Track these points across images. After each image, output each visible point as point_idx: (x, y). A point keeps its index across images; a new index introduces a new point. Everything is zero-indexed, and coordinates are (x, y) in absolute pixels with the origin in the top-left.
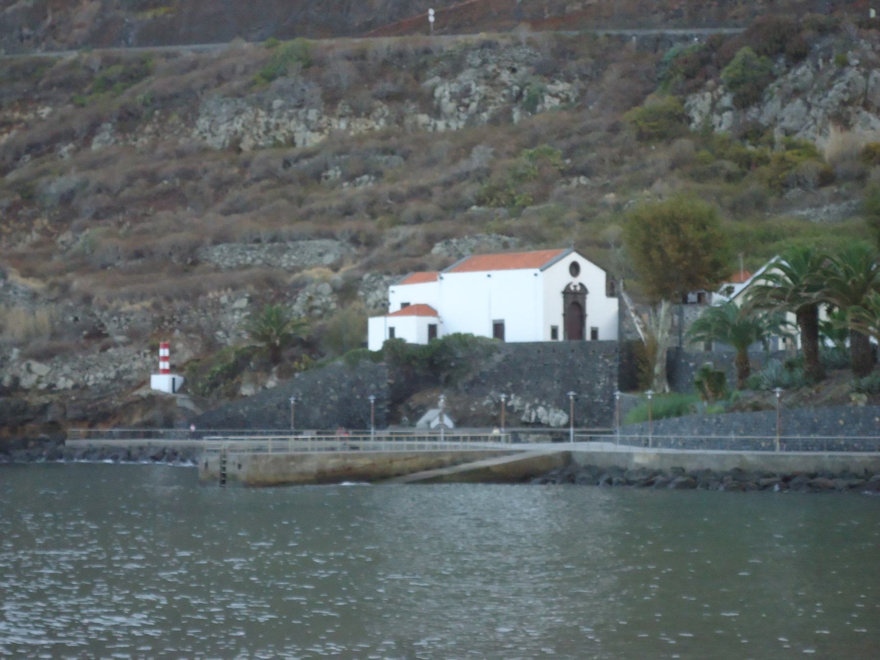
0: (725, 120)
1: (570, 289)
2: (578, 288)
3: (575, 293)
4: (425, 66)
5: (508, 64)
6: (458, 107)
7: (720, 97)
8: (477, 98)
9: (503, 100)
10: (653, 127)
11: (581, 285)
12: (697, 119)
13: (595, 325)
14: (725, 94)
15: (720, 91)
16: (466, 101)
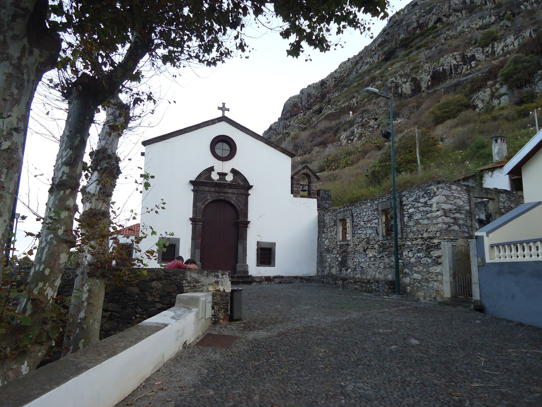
0: (502, 102)
1: (209, 177)
2: (229, 178)
3: (221, 185)
4: (338, 129)
5: (373, 117)
6: (347, 141)
7: (497, 89)
8: (357, 135)
9: (369, 134)
10: (445, 112)
11: (234, 171)
12: (480, 105)
13: (267, 239)
14: (502, 87)
15: (497, 86)
16: (352, 138)
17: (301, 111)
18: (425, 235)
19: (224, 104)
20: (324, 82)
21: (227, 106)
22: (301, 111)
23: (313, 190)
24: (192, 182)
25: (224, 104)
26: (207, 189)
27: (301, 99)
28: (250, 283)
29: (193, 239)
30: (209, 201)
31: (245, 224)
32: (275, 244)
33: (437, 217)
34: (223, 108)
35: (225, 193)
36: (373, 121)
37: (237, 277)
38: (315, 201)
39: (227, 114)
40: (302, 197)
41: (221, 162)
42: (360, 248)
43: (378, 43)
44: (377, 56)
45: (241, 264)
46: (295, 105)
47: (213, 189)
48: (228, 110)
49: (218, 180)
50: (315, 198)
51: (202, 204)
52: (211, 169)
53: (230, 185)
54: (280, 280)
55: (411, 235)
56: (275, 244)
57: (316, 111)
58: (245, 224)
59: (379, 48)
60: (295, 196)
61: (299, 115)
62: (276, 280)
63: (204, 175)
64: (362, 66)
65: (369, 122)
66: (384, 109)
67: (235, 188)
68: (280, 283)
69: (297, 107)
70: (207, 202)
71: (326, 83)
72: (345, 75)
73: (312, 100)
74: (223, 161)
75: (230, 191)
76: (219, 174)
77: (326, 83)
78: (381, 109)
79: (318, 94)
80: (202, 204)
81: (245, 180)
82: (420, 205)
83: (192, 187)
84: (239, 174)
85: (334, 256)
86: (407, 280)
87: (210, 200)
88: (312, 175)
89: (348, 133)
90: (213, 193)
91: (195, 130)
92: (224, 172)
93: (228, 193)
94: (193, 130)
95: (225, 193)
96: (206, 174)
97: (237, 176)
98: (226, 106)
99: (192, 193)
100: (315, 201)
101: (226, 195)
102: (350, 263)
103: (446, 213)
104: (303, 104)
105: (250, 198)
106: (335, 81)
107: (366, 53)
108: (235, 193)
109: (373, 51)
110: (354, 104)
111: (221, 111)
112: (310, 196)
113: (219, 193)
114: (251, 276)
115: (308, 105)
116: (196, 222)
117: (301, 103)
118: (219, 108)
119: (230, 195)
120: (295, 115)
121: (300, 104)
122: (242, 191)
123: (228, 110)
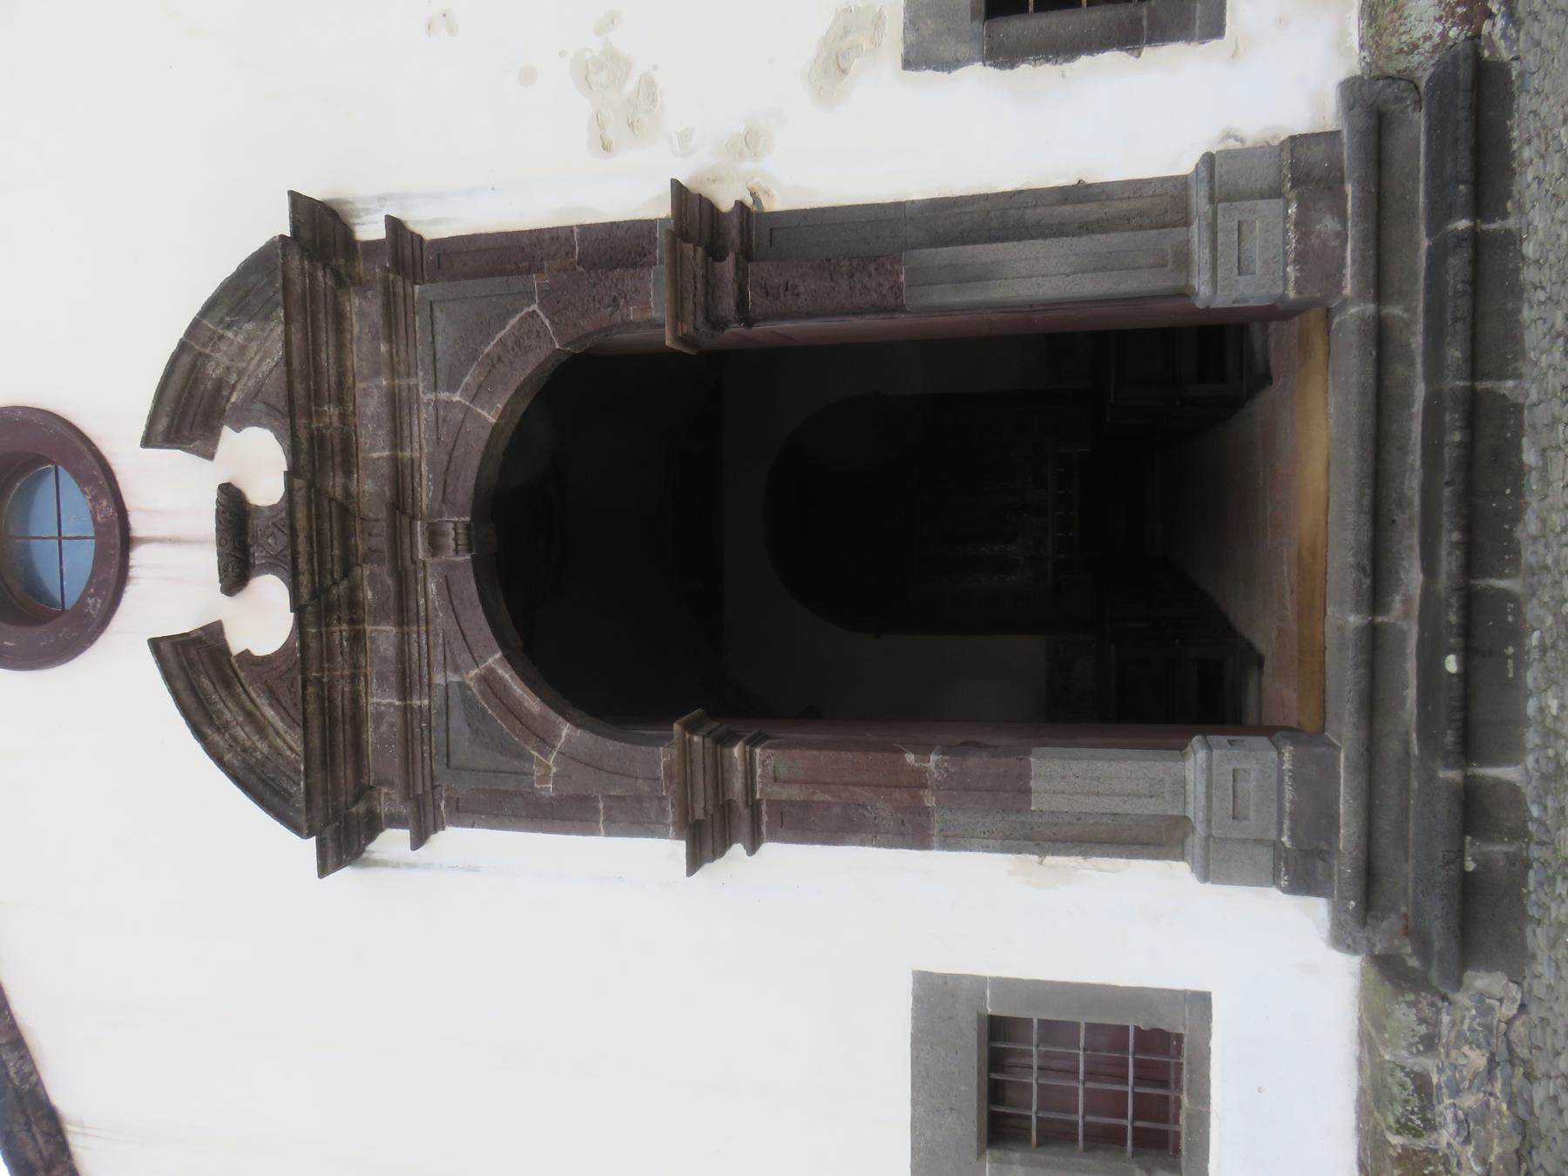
26: (381, 699)
30: (506, 674)
31: (715, 252)
35: (400, 504)
37: (1379, 284)
41: (138, 556)
47: (383, 636)
51: (545, 741)
58: (715, 252)
63: (260, 727)
67: (342, 394)
70: (518, 688)
74: (126, 542)
75: (375, 449)
76: (235, 576)
80: (545, 741)
83: (392, 842)
87: (495, 660)
90: (416, 633)
93: (400, 476)
95: (400, 504)
101: (426, 493)
114: (1353, 91)
116: (725, 809)
119: (421, 447)
122: (362, 310)
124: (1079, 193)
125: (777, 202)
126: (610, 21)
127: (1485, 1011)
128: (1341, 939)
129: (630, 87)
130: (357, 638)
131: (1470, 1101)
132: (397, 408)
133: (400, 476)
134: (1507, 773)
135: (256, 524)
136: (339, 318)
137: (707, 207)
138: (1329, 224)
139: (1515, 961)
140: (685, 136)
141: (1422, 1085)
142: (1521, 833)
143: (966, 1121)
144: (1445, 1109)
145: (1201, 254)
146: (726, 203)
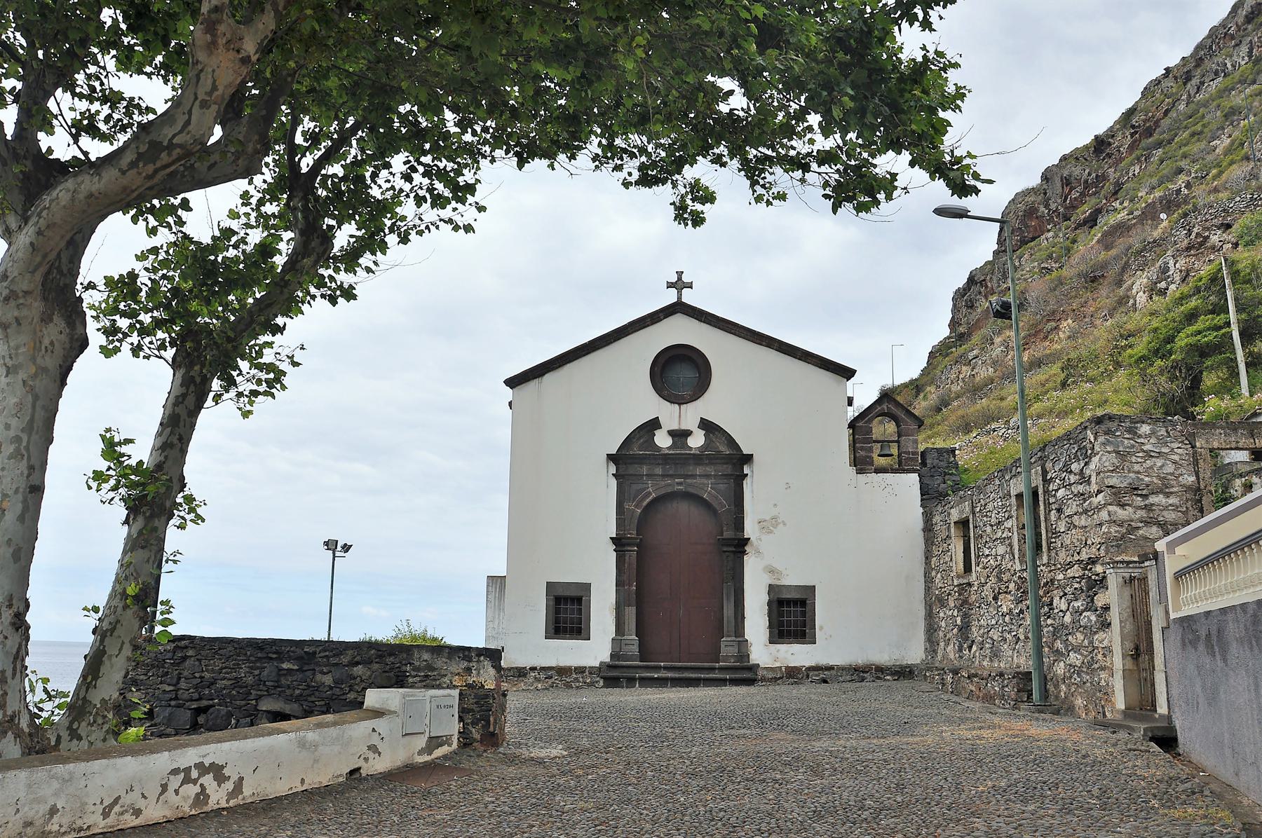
2: (697, 441)
3: (679, 459)
8: (1177, 278)
11: (707, 426)
13: (793, 578)
16: (1163, 285)
17: (1049, 227)
18: (1084, 556)
19: (680, 274)
20: (1102, 141)
21: (685, 279)
22: (1049, 227)
23: (908, 453)
24: (610, 457)
25: (680, 274)
27: (1045, 194)
28: (750, 682)
29: (619, 584)
32: (812, 589)
33: (1099, 508)
34: (679, 284)
36: (1219, 232)
37: (721, 669)
38: (914, 477)
39: (689, 297)
40: (878, 471)
41: (677, 406)
42: (987, 592)
43: (1244, 13)
44: (1244, 49)
45: (729, 639)
46: (1031, 212)
47: (659, 471)
48: (690, 286)
49: (669, 448)
50: (914, 471)
51: (636, 506)
52: (654, 424)
53: (698, 458)
54: (822, 674)
55: (1062, 556)
56: (812, 589)
57: (1085, 222)
59: (1250, 27)
60: (860, 472)
61: (1043, 237)
62: (814, 676)
64: (1203, 83)
65: (1208, 237)
66: (1249, 196)
67: (711, 464)
68: (825, 681)
69: (1037, 217)
70: (648, 500)
71: (1110, 144)
72: (1159, 114)
73: (1074, 195)
74: (680, 404)
76: (672, 433)
77: (1110, 144)
78: (1238, 199)
79: (1089, 174)
81: (731, 442)
82: (1073, 478)
83: (613, 469)
84: (717, 430)
85: (950, 613)
86: (1060, 669)
88: (902, 415)
89: (1153, 272)
91: (615, 341)
92: (684, 427)
94: (612, 343)
95: (686, 477)
96: (640, 438)
97: (714, 434)
98: (685, 279)
99: (613, 483)
100: (914, 477)
101: (689, 481)
102: (975, 633)
103: (1118, 497)
104: (1053, 207)
105: (747, 484)
106: (1132, 135)
107: (1211, 47)
108: (711, 475)
109: (1232, 37)
110: (1179, 191)
111: (674, 291)
112: (901, 468)
113: (671, 476)
115: (1066, 208)
116: (624, 545)
117: (1047, 206)
118: (670, 285)
119: (698, 480)
120: (1033, 239)
121: (1042, 208)
123: (690, 286)
124: (743, 618)
125: (746, 558)
126: (785, 524)
127: (597, 682)
128: (601, 663)
129: (771, 528)
130: (659, 464)
131: (581, 680)
132: (708, 476)
133: (693, 476)
134: (637, 685)
135: (683, 439)
136: (727, 464)
137: (746, 544)
138: (732, 661)
139: (606, 686)
140: (760, 539)
141: (584, 672)
142: (627, 687)
143: (561, 593)
144: (580, 676)
145: (729, 639)
146: (746, 548)
